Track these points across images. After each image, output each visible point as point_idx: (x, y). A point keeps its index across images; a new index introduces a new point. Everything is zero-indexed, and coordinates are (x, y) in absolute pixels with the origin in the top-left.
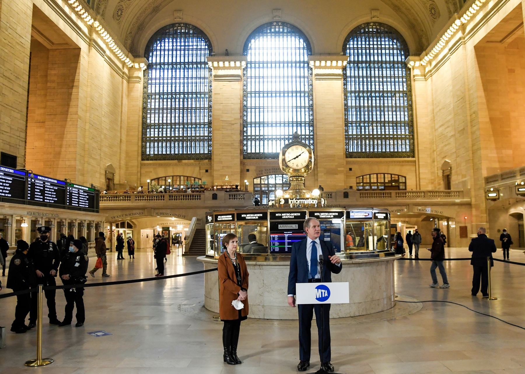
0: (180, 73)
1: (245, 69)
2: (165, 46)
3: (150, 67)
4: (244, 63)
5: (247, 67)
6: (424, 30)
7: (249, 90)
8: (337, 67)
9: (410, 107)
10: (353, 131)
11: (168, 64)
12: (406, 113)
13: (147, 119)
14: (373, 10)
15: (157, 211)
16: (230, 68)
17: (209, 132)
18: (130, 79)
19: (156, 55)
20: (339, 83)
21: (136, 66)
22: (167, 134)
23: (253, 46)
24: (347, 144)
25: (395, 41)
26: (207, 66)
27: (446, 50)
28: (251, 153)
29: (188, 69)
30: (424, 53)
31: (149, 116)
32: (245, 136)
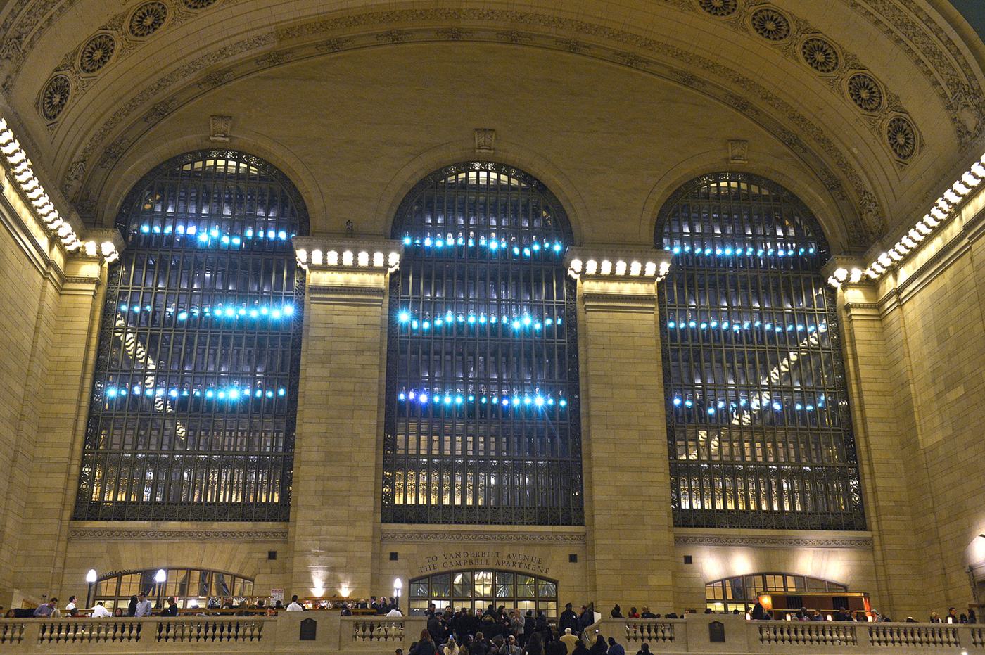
6: (869, 188)
16: (355, 269)
20: (650, 319)
21: (90, 248)
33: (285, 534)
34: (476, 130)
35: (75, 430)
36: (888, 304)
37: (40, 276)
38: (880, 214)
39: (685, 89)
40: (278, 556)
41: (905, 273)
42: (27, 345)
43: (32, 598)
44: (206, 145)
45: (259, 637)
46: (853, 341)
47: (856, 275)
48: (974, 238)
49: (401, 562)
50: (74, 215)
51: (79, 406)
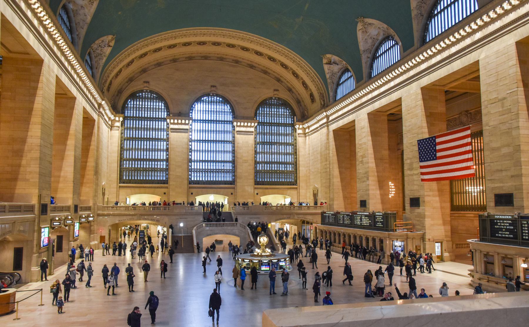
1: (191, 125)
4: (191, 121)
7: (193, 139)
8: (251, 127)
9: (295, 153)
10: (260, 167)
14: (275, 90)
16: (181, 124)
17: (167, 166)
18: (111, 127)
20: (252, 137)
21: (117, 119)
23: (196, 109)
27: (317, 125)
28: (194, 180)
30: (305, 121)
34: (212, 86)
41: (311, 129)
47: (301, 127)
48: (321, 129)
50: (114, 113)
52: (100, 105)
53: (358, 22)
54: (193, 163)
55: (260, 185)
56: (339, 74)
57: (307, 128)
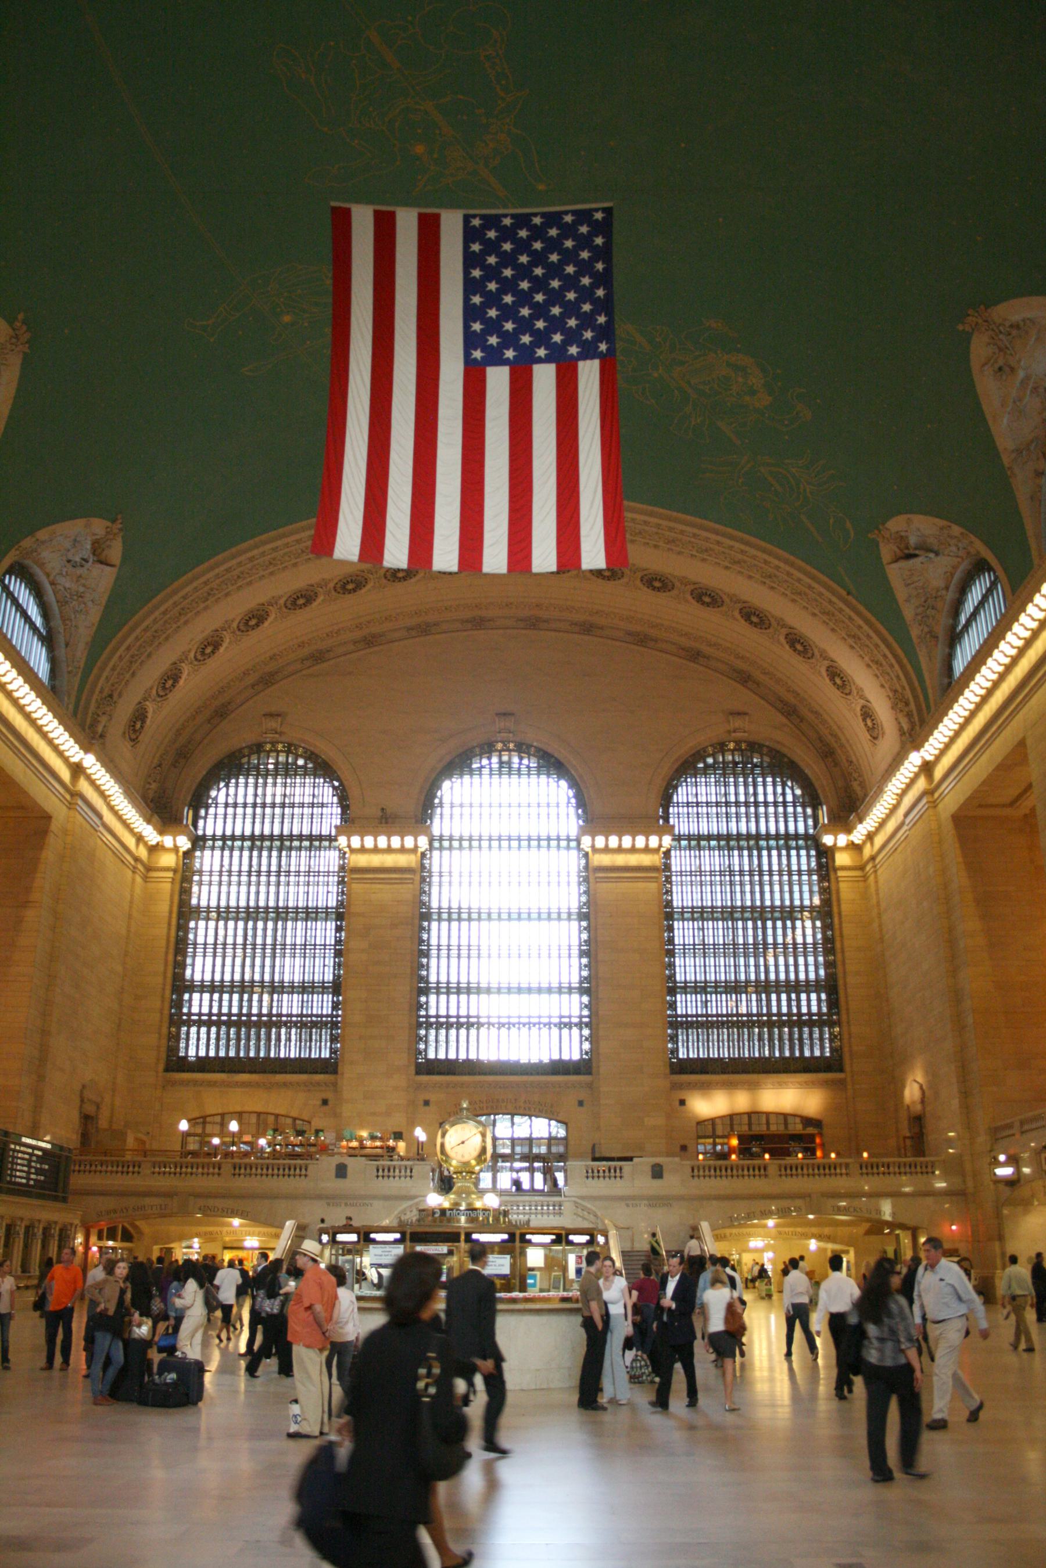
0: (269, 860)
2: (236, 795)
3: (199, 842)
4: (423, 842)
5: (431, 848)
8: (647, 850)
10: (687, 1005)
11: (243, 838)
12: (821, 959)
13: (184, 969)
15: (201, 1202)
17: (335, 1006)
19: (216, 814)
21: (168, 841)
22: (230, 1006)
23: (446, 800)
24: (674, 1039)
25: (789, 783)
26: (334, 844)
28: (436, 1060)
29: (291, 849)
31: (189, 961)
32: (423, 1017)
33: (335, 1084)
34: (497, 714)
35: (163, 997)
36: (868, 868)
37: (130, 873)
38: (862, 785)
39: (692, 664)
40: (330, 1103)
41: (879, 841)
42: (124, 932)
43: (140, 1135)
44: (263, 740)
45: (306, 1176)
46: (839, 900)
49: (432, 1107)
50: (156, 818)
51: (165, 977)
52: (77, 770)
53: (967, 338)
54: (433, 998)
55: (692, 1072)
56: (950, 595)
57: (864, 842)
